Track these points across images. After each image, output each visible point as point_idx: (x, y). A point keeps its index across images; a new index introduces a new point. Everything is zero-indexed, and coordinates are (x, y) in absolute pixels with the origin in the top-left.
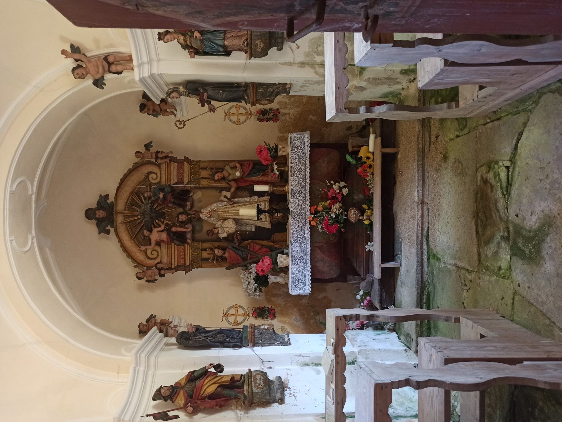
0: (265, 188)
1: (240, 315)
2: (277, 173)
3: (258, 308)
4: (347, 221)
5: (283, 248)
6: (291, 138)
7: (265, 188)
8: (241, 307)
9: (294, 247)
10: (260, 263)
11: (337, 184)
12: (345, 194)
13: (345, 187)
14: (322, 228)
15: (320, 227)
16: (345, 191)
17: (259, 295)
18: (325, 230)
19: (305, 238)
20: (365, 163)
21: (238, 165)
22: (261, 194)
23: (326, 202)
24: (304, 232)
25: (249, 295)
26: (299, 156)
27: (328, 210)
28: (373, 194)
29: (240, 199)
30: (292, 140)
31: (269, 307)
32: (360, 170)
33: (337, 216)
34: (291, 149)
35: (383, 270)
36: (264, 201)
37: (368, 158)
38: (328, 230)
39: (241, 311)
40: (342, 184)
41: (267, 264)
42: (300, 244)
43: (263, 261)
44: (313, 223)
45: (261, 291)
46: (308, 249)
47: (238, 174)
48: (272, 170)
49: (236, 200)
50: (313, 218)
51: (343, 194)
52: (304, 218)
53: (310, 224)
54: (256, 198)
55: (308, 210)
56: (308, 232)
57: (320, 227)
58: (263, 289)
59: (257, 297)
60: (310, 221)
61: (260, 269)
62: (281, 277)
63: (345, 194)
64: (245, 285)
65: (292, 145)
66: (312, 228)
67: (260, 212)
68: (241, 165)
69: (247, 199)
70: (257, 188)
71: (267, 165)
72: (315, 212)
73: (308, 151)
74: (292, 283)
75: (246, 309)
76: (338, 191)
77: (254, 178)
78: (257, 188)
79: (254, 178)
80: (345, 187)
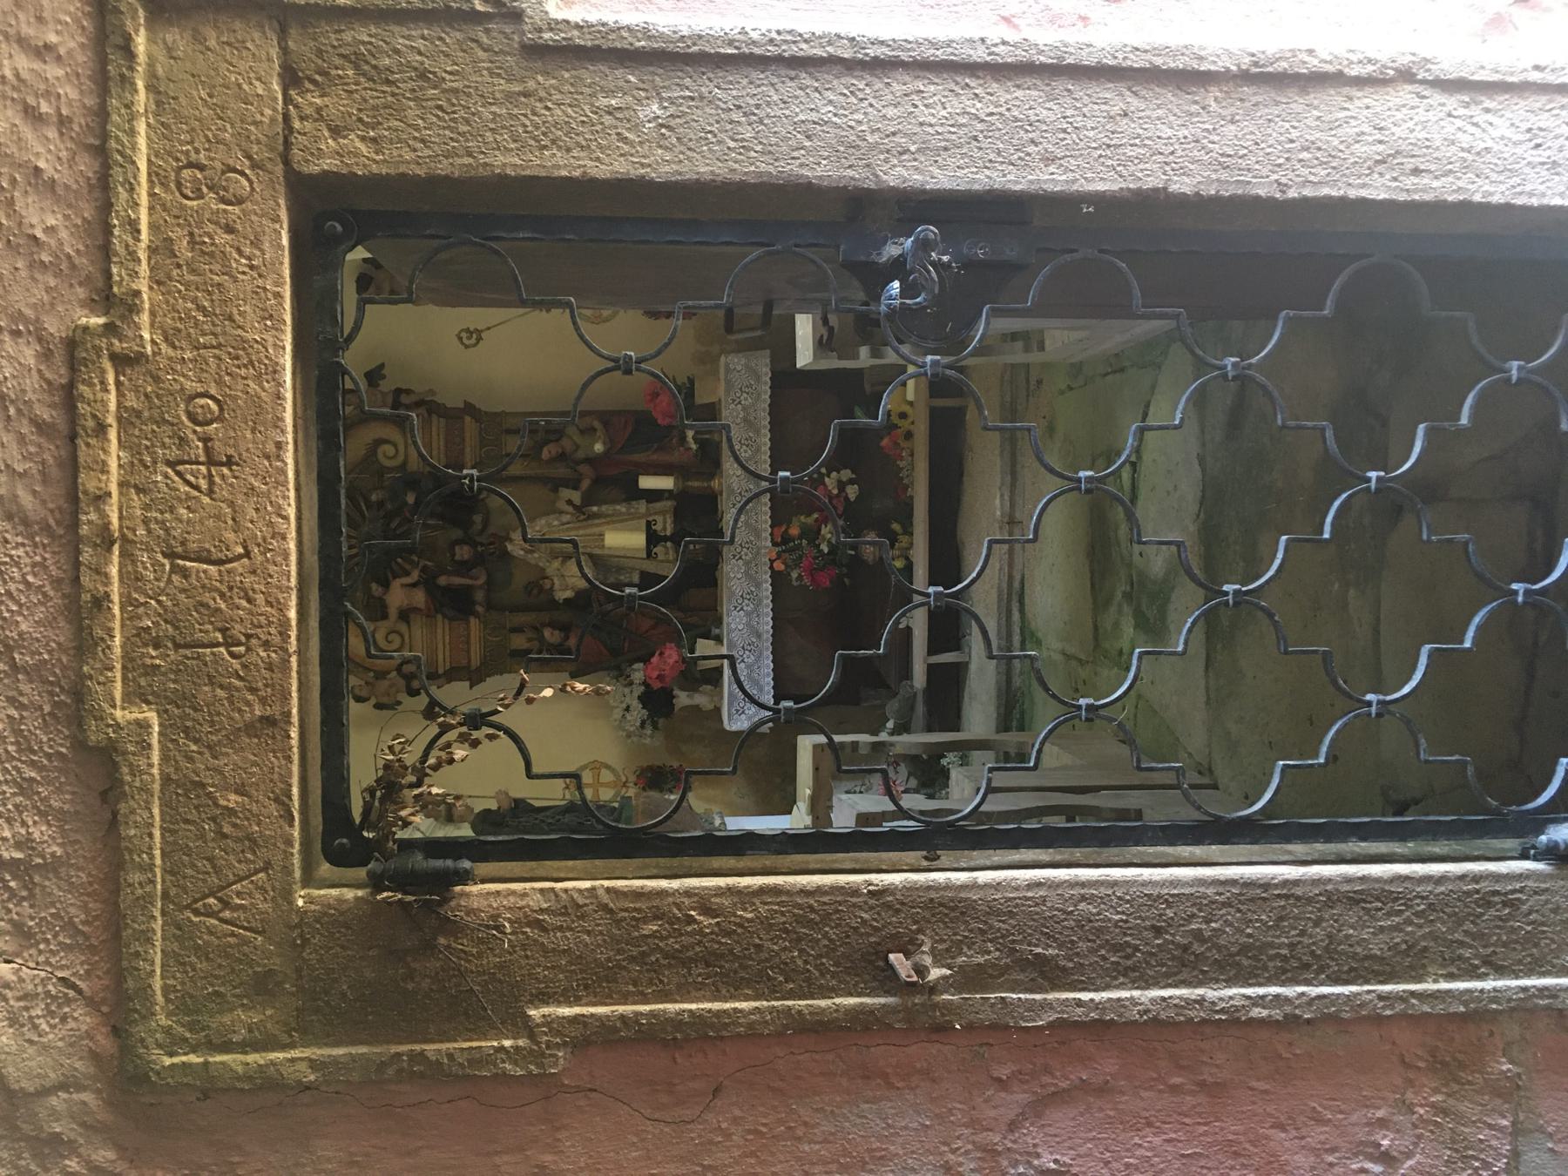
0: (665, 483)
1: (606, 785)
2: (694, 447)
3: (650, 768)
4: (857, 560)
5: (708, 623)
6: (727, 365)
7: (665, 483)
8: (608, 767)
9: (734, 622)
10: (655, 660)
11: (834, 474)
12: (852, 497)
13: (851, 482)
14: (800, 577)
15: (794, 575)
16: (852, 492)
17: (652, 737)
18: (807, 581)
19: (760, 601)
20: (896, 427)
21: (596, 424)
22: (654, 495)
23: (809, 515)
24: (758, 585)
25: (629, 736)
26: (744, 409)
27: (812, 534)
28: (912, 498)
29: (604, 508)
30: (728, 370)
31: (676, 765)
32: (885, 442)
33: (834, 549)
34: (728, 391)
35: (931, 669)
36: (663, 513)
37: (903, 416)
38: (813, 580)
39: (606, 776)
40: (846, 474)
41: (671, 661)
42: (748, 614)
43: (661, 654)
44: (779, 566)
45: (655, 727)
46: (767, 624)
47: (599, 447)
48: (683, 439)
49: (595, 509)
50: (779, 556)
51: (847, 498)
52: (758, 553)
53: (771, 567)
54: (642, 506)
55: (766, 534)
56: (767, 587)
57: (794, 575)
58: (661, 721)
59: (648, 741)
60: (772, 562)
61: (656, 674)
62: (705, 693)
63: (852, 497)
64: (618, 713)
65: (728, 382)
66: (776, 577)
67: (653, 539)
68: (606, 424)
69: (622, 508)
70: (646, 482)
71: (670, 427)
72: (782, 542)
73: (766, 397)
74: (730, 704)
75: (619, 768)
76: (835, 492)
77: (637, 457)
78: (646, 482)
79: (637, 457)
80: (851, 482)
